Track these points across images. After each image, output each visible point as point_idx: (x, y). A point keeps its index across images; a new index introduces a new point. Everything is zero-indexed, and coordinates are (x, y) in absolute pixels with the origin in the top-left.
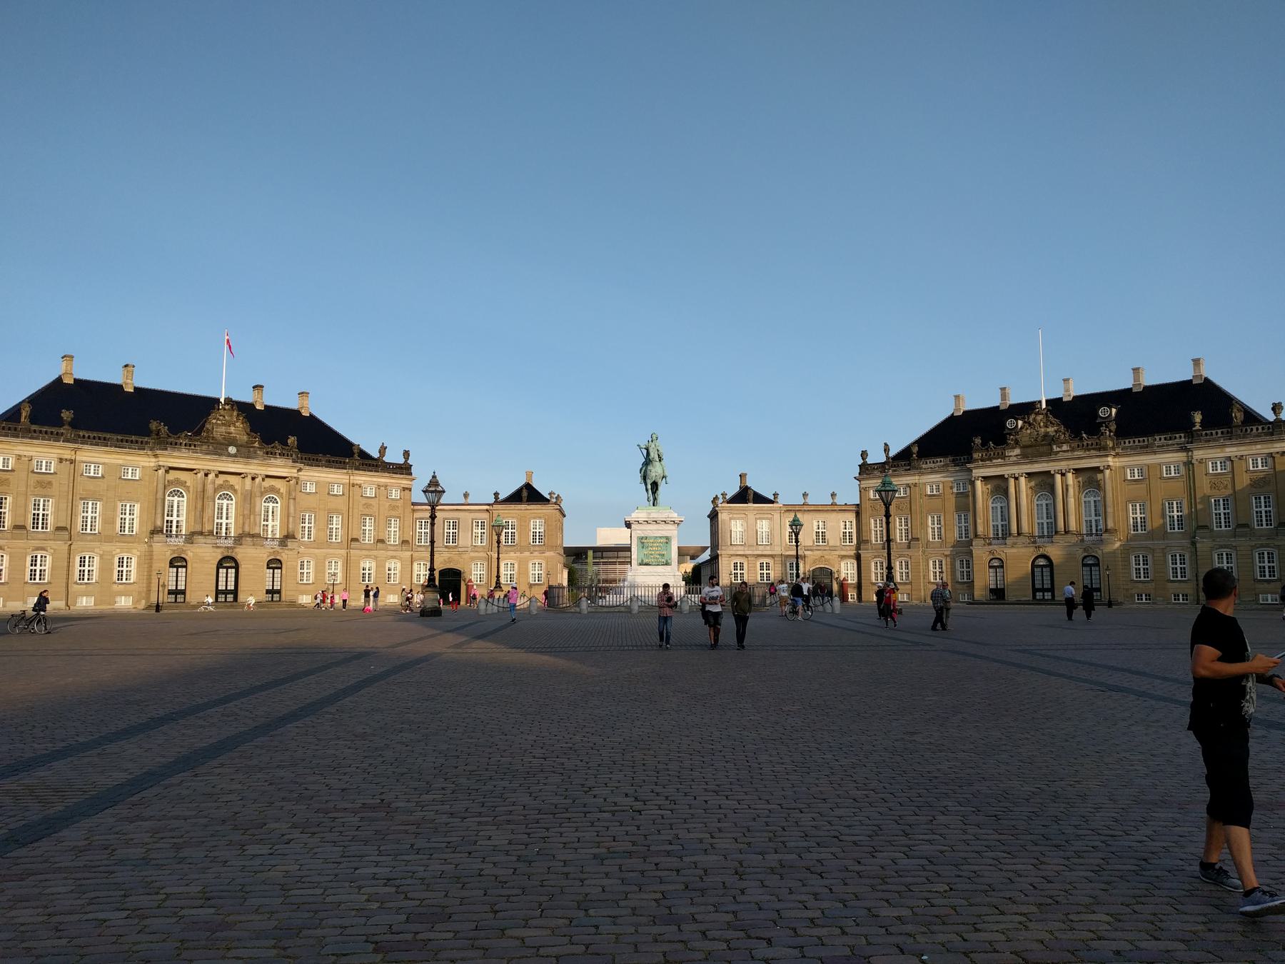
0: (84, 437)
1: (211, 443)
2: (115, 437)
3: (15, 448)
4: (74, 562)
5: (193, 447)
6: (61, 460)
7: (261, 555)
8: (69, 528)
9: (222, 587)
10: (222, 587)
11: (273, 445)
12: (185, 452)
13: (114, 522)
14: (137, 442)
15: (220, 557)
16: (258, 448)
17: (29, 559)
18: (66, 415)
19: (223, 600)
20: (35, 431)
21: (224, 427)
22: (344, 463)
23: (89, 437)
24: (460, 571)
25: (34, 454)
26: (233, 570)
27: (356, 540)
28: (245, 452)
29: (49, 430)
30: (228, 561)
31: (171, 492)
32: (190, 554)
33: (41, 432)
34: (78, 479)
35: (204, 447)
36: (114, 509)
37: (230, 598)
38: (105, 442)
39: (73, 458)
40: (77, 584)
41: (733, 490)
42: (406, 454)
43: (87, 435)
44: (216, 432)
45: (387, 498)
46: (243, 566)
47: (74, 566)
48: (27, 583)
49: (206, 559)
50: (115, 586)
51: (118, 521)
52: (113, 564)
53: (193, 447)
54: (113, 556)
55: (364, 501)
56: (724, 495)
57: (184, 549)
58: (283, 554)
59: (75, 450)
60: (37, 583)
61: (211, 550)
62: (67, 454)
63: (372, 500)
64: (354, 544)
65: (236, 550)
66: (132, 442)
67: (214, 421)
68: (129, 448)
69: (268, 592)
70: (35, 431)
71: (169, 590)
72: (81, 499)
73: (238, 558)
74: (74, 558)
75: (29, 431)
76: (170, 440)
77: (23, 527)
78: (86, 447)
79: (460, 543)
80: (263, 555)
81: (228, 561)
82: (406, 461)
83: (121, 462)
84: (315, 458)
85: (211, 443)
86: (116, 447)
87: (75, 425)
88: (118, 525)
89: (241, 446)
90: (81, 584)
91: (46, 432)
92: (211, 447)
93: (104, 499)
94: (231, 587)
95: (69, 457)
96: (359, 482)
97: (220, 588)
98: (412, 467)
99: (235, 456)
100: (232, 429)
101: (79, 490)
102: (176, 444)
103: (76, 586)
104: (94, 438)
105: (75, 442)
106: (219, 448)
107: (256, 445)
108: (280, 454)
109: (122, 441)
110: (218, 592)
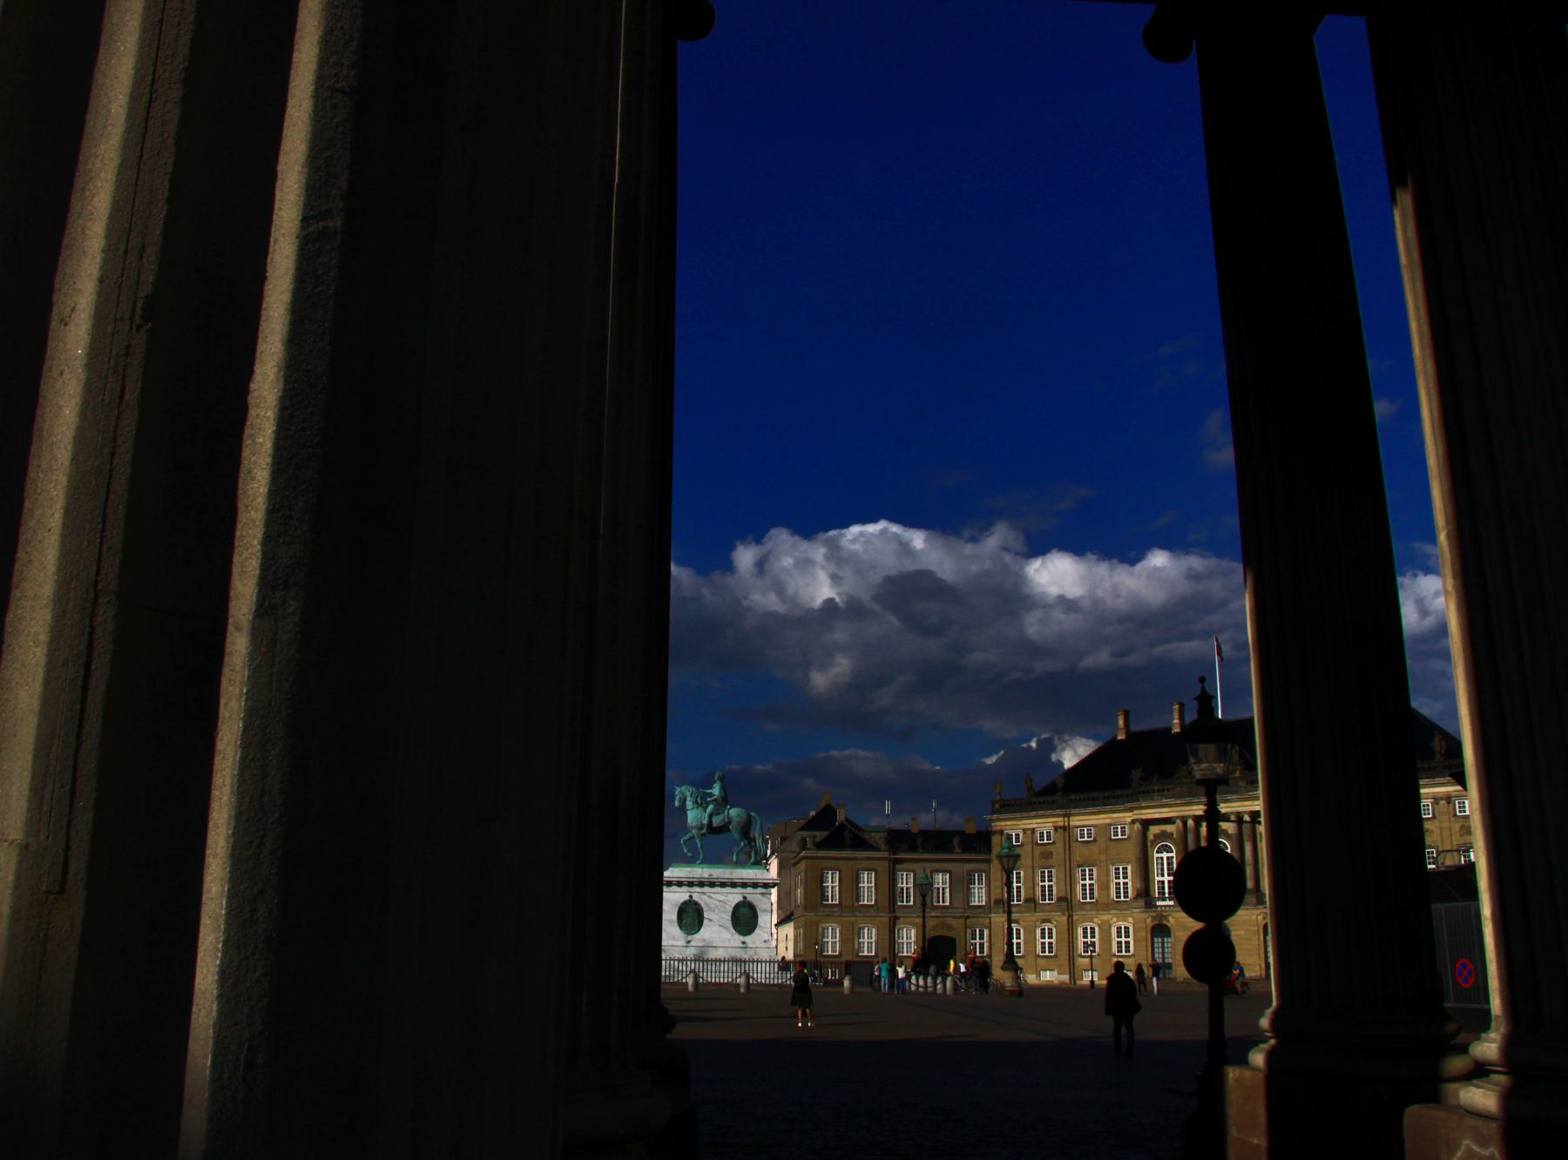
3: (1020, 823)
4: (1077, 934)
5: (1166, 792)
14: (1122, 796)
17: (1038, 932)
20: (1035, 803)
23: (1080, 800)
25: (1034, 826)
31: (1159, 848)
32: (1171, 920)
34: (1074, 845)
36: (1108, 875)
43: (1078, 798)
46: (1233, 933)
47: (1077, 938)
48: (1038, 956)
52: (1110, 935)
53: (1166, 792)
54: (1110, 927)
57: (1164, 914)
59: (1068, 816)
62: (1060, 821)
72: (1079, 866)
74: (1077, 930)
76: (1142, 788)
83: (1108, 821)
90: (1084, 957)
93: (1098, 863)
101: (1077, 858)
102: (1148, 792)
103: (1081, 960)
107: (1237, 774)
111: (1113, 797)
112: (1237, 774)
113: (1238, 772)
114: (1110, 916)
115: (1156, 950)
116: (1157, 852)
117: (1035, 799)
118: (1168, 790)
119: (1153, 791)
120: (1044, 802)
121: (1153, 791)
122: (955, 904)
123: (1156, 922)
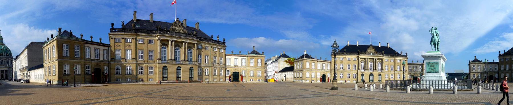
6: (344, 58)
9: (370, 79)
12: (363, 55)
13: (352, 68)
18: (345, 50)
27: (396, 70)
28: (374, 54)
30: (371, 74)
35: (366, 54)
37: (372, 81)
38: (351, 54)
41: (473, 59)
55: (398, 63)
56: (471, 60)
64: (396, 71)
69: (379, 80)
73: (373, 74)
77: (339, 69)
78: (348, 55)
80: (378, 74)
81: (371, 74)
87: (346, 52)
94: (372, 79)
99: (372, 55)
100: (372, 50)
105: (346, 55)
106: (369, 54)
107: (376, 53)
110: (370, 80)
112: (376, 53)
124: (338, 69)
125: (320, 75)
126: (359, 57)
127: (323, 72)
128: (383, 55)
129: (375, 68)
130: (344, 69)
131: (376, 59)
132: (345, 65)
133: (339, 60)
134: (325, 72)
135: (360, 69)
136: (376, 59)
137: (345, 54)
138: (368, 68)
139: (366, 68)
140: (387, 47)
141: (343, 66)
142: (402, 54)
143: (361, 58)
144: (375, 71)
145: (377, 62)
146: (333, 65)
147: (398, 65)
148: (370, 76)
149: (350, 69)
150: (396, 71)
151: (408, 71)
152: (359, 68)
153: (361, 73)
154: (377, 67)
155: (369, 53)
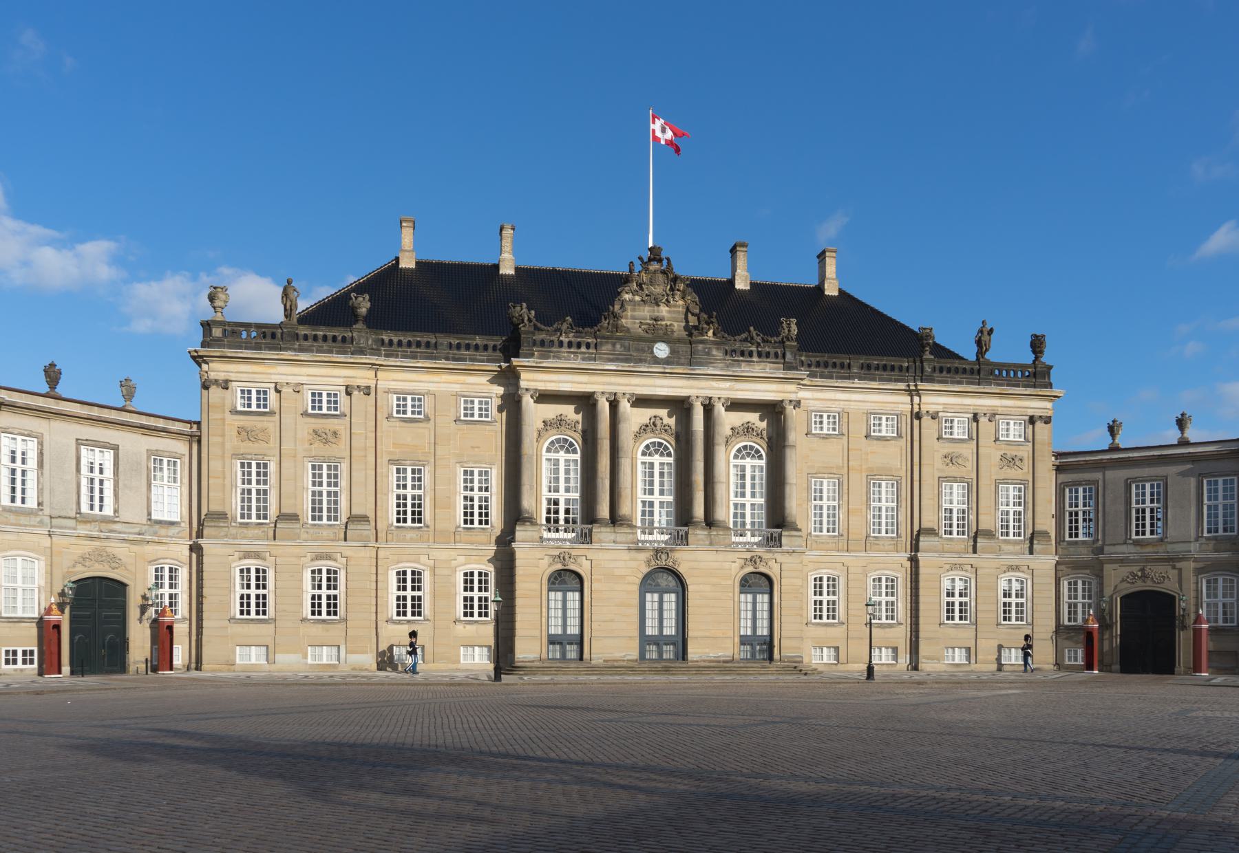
0: (391, 343)
1: (619, 339)
2: (444, 340)
5: (583, 349)
7: (727, 565)
8: (371, 516)
9: (651, 631)
10: (651, 631)
11: (744, 336)
14: (486, 348)
15: (645, 570)
16: (713, 343)
18: (363, 305)
19: (655, 656)
20: (306, 338)
21: (647, 308)
22: (901, 369)
23: (400, 344)
24: (1174, 597)
26: (673, 597)
29: (330, 334)
33: (315, 338)
34: (383, 424)
35: (606, 348)
37: (669, 652)
38: (430, 351)
39: (372, 383)
40: (394, 622)
42: (1037, 345)
43: (395, 340)
44: (633, 318)
45: (997, 440)
49: (617, 572)
50: (460, 627)
51: (460, 504)
53: (583, 349)
58: (772, 563)
60: (324, 621)
61: (626, 555)
63: (964, 445)
65: (677, 555)
66: (477, 348)
67: (627, 297)
68: (472, 360)
70: (306, 338)
71: (549, 636)
72: (391, 462)
73: (682, 569)
75: (297, 337)
78: (392, 361)
79: (1172, 533)
80: (733, 566)
82: (1036, 358)
83: (456, 388)
84: (838, 361)
85: (619, 339)
86: (447, 359)
87: (375, 321)
88: (460, 511)
89: (679, 341)
91: (325, 338)
92: (618, 346)
94: (670, 629)
95: (363, 383)
96: (932, 409)
97: (649, 632)
98: (1052, 372)
99: (666, 362)
104: (409, 344)
105: (375, 352)
108: (760, 355)
109: (458, 347)
110: (645, 640)
111: (468, 347)
113: (710, 333)
114: (453, 553)
115: (552, 613)
116: (548, 450)
117: (303, 330)
118: (588, 346)
119: (561, 344)
120: (334, 339)
121: (561, 344)
122: (125, 515)
123: (559, 566)
124: (282, 517)
125: (39, 579)
126: (531, 380)
127: (87, 547)
128: (788, 367)
129: (699, 511)
130: (352, 518)
131: (708, 409)
132: (363, 475)
133: (287, 419)
134: (120, 550)
135: (531, 520)
136: (708, 409)
137: (361, 352)
138: (625, 509)
139: (604, 511)
140: (820, 289)
141: (343, 482)
142: (990, 356)
143: (545, 397)
144: (698, 535)
145: (720, 440)
146: (215, 465)
147: (952, 470)
148: (652, 599)
149: (418, 516)
150: (924, 542)
151: (1060, 539)
152: (527, 503)
153: (546, 567)
154: (719, 491)
155: (629, 336)
